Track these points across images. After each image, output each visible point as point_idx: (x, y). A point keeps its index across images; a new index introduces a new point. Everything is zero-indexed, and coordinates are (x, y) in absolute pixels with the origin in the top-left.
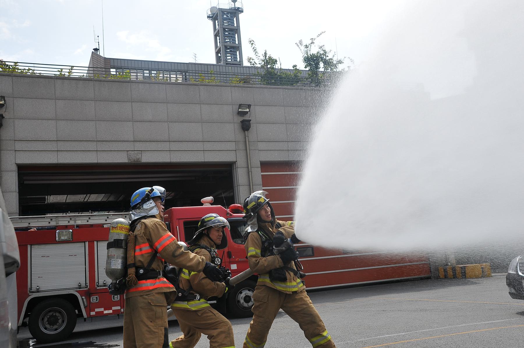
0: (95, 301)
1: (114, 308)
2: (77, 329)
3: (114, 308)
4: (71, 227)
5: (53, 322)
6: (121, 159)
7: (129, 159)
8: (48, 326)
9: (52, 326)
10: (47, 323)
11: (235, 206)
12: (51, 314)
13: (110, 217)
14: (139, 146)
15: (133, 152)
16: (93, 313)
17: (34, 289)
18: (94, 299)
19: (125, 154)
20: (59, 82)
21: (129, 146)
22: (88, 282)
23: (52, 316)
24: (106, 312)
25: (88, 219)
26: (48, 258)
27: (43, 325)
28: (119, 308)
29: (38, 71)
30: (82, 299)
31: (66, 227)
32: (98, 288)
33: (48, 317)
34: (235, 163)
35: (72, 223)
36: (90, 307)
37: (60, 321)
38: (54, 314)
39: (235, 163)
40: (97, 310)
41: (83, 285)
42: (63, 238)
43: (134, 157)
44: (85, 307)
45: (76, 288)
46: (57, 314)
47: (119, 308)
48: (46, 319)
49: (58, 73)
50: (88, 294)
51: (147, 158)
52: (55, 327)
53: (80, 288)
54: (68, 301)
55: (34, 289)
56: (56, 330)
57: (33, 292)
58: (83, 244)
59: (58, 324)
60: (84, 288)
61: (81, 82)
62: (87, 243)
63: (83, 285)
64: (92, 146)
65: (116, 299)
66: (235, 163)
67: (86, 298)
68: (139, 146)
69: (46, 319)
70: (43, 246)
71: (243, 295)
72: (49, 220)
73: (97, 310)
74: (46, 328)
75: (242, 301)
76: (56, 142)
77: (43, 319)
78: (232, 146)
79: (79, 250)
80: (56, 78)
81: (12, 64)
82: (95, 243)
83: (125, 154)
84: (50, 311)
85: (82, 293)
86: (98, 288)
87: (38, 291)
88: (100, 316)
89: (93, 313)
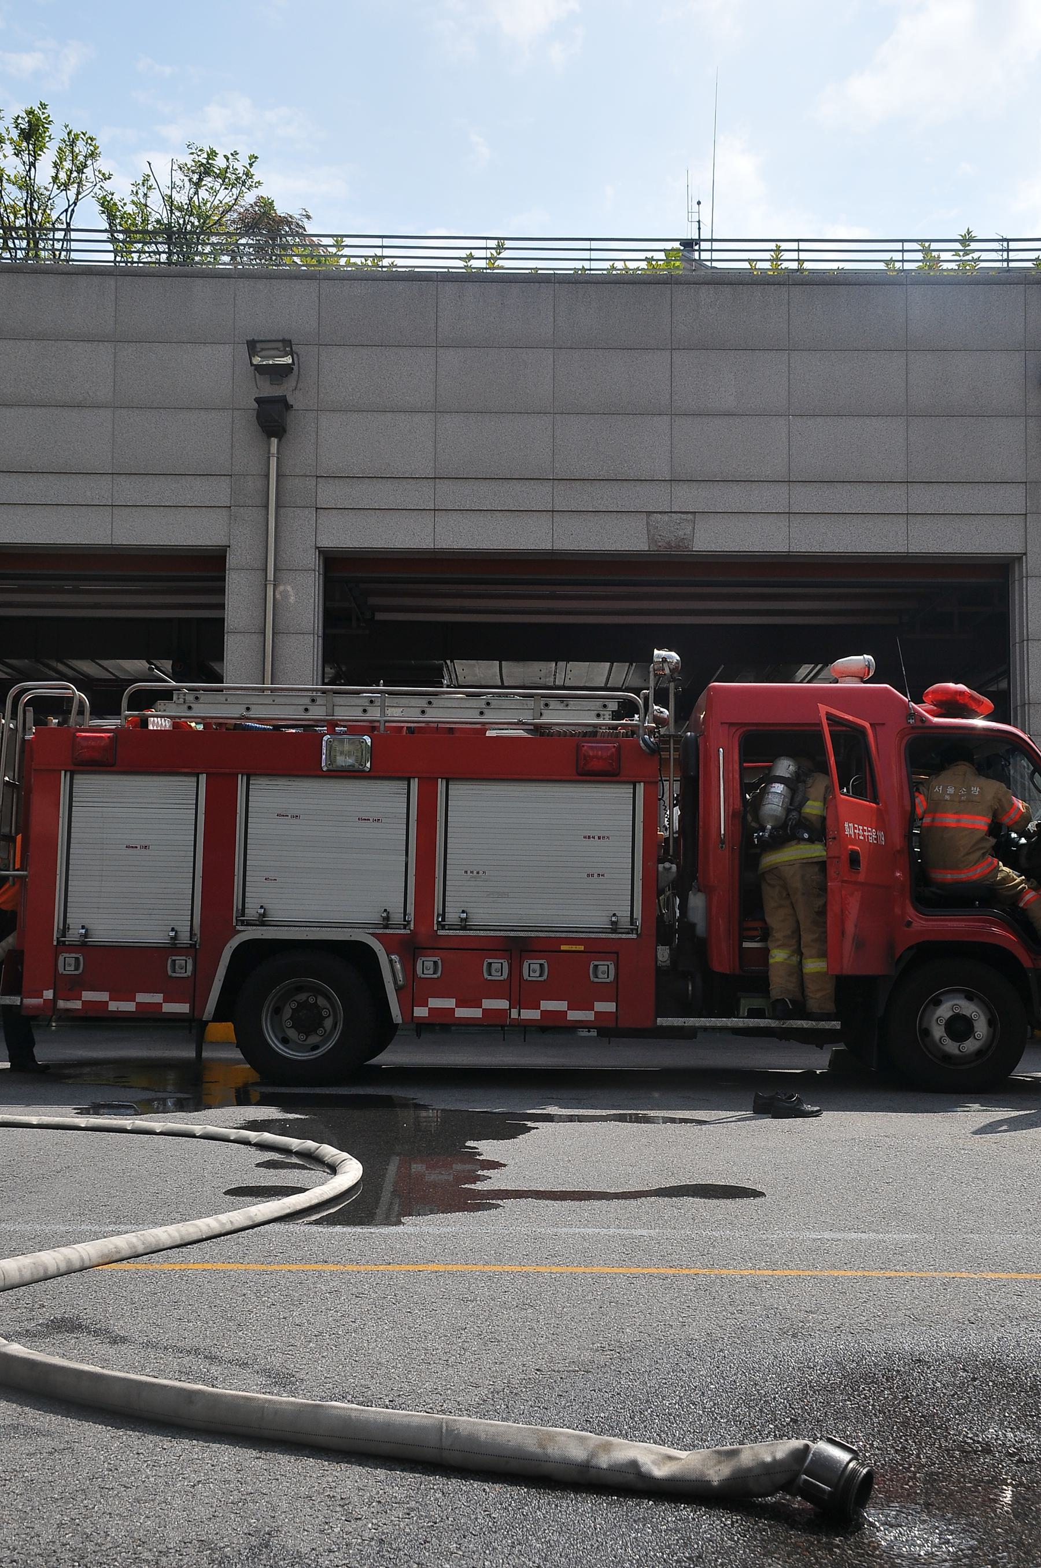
0: (429, 973)
1: (488, 1004)
2: (387, 1058)
3: (488, 1004)
4: (371, 729)
5: (308, 1022)
6: (627, 538)
7: (651, 539)
8: (292, 1034)
9: (303, 1037)
10: (289, 1024)
11: (947, 691)
12: (302, 997)
13: (494, 703)
14: (686, 497)
15: (666, 517)
16: (421, 1012)
17: (252, 912)
18: (426, 967)
19: (638, 524)
20: (450, 288)
21: (655, 498)
22: (411, 909)
23: (302, 1006)
24: (462, 1013)
25: (422, 702)
26: (295, 821)
27: (278, 1027)
28: (503, 1004)
29: (405, 262)
30: (391, 961)
31: (355, 729)
32: (441, 932)
33: (294, 1005)
34: (1018, 559)
35: (374, 714)
36: (413, 991)
37: (328, 1023)
38: (311, 1000)
39: (1020, 559)
40: (434, 1003)
41: (397, 917)
42: (342, 761)
43: (671, 533)
44: (398, 989)
45: (376, 925)
46: (321, 1001)
47: (503, 1004)
48: (287, 1012)
49: (461, 264)
50: (410, 948)
51: (710, 539)
52: (313, 1039)
53: (386, 927)
54: (342, 962)
55: (252, 912)
56: (315, 1048)
57: (249, 924)
58: (404, 785)
59: (320, 1031)
60: (397, 926)
61: (515, 289)
62: (415, 784)
63: (397, 917)
64: (538, 496)
65: (496, 976)
66: (1018, 559)
67: (401, 961)
68: (686, 497)
69: (287, 1012)
70: (282, 783)
71: (944, 1011)
72: (307, 701)
73: (434, 1003)
74: (285, 1041)
75: (938, 1032)
76: (431, 482)
77: (277, 1011)
78: (1013, 499)
79: (390, 802)
80: (448, 278)
81: (330, 241)
82: (441, 785)
83: (638, 524)
84: (299, 989)
85: (391, 944)
86: (441, 932)
87: (262, 921)
88: (441, 1027)
89: (421, 1012)
